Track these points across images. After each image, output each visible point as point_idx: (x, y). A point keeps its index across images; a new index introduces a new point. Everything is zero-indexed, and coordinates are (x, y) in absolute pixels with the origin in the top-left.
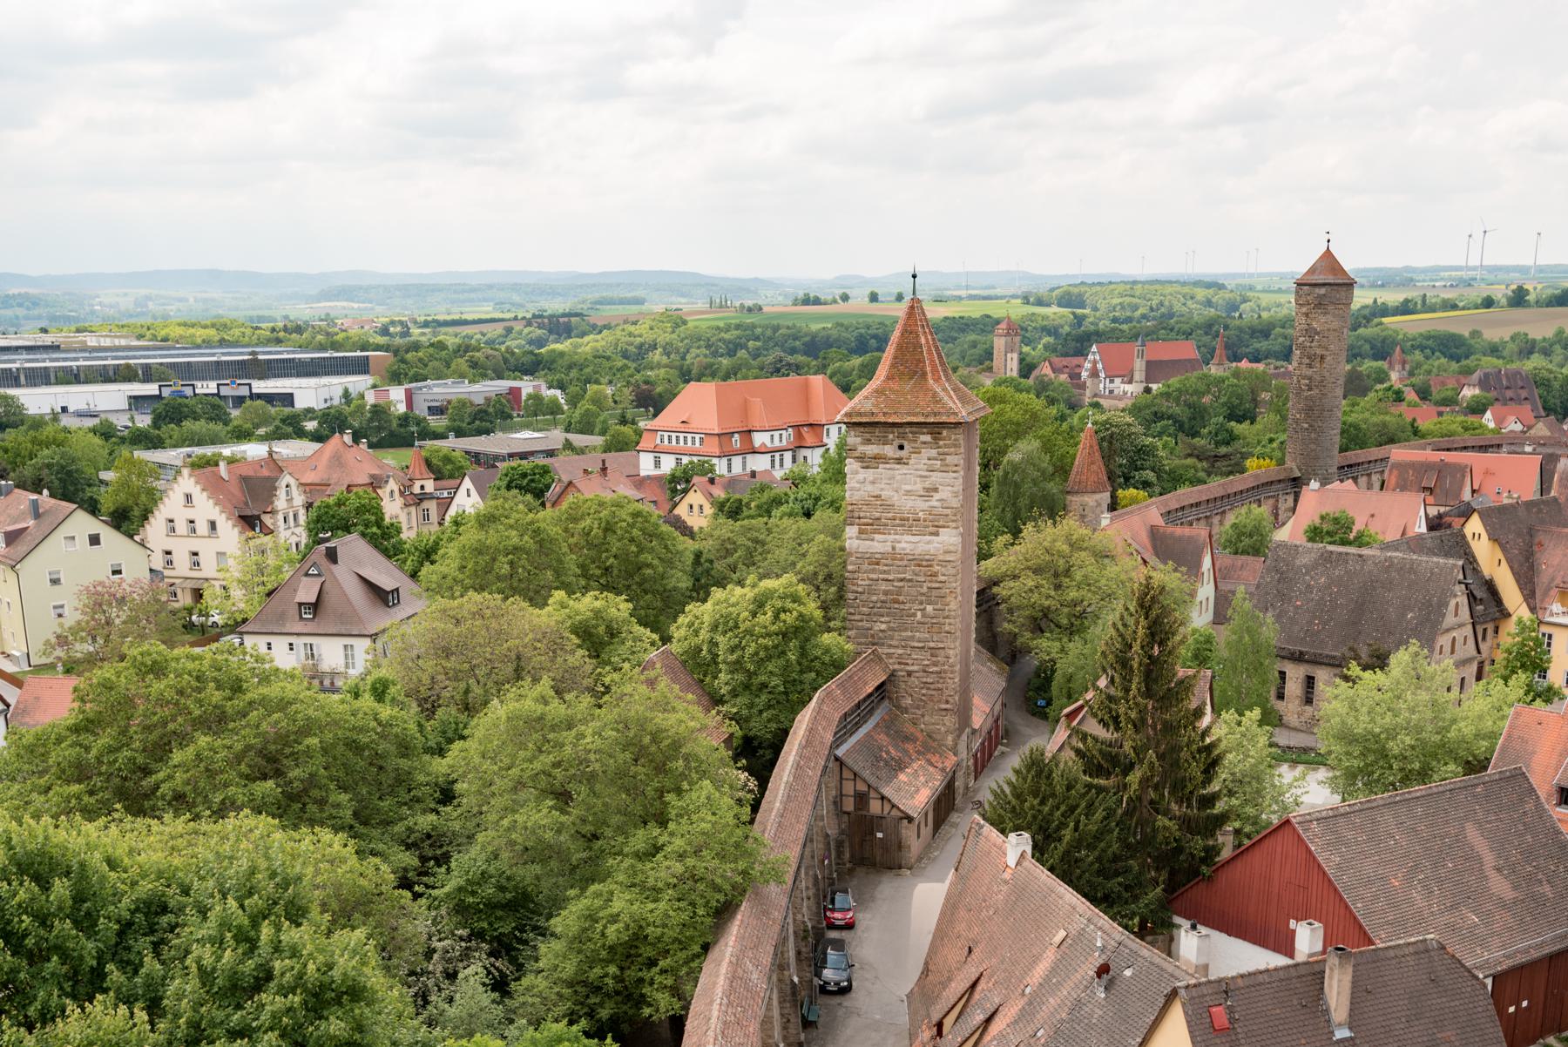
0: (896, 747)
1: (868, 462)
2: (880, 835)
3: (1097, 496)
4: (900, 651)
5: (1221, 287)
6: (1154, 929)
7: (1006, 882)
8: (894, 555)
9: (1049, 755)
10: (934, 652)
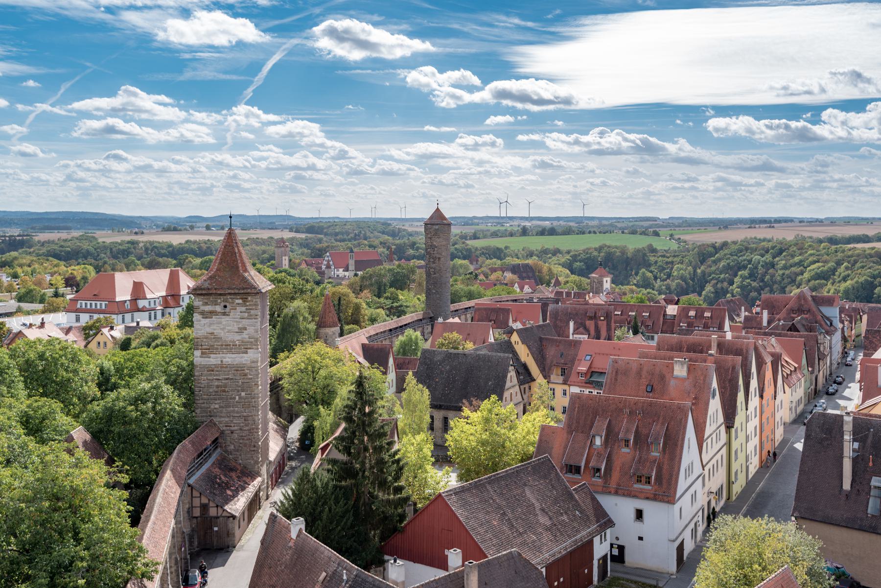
0: (225, 476)
1: (206, 315)
2: (216, 529)
3: (333, 329)
4: (227, 419)
5: (390, 225)
6: (375, 562)
7: (291, 547)
8: (222, 366)
9: (312, 471)
10: (246, 418)
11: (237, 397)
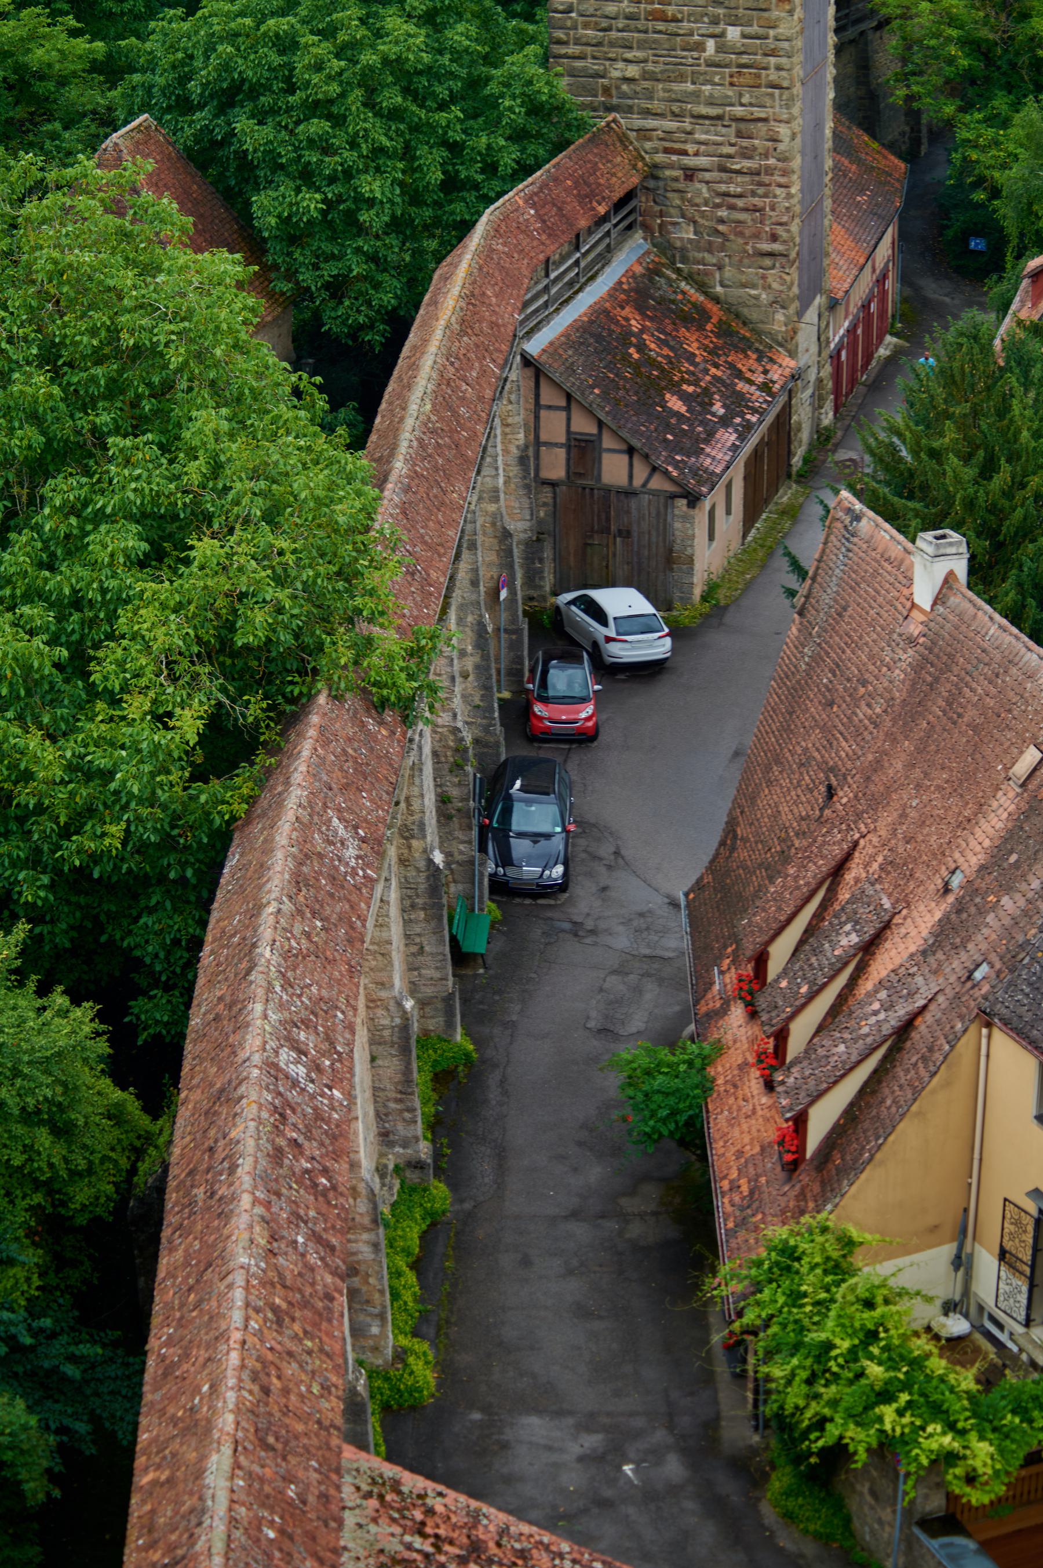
11: (711, 45)
